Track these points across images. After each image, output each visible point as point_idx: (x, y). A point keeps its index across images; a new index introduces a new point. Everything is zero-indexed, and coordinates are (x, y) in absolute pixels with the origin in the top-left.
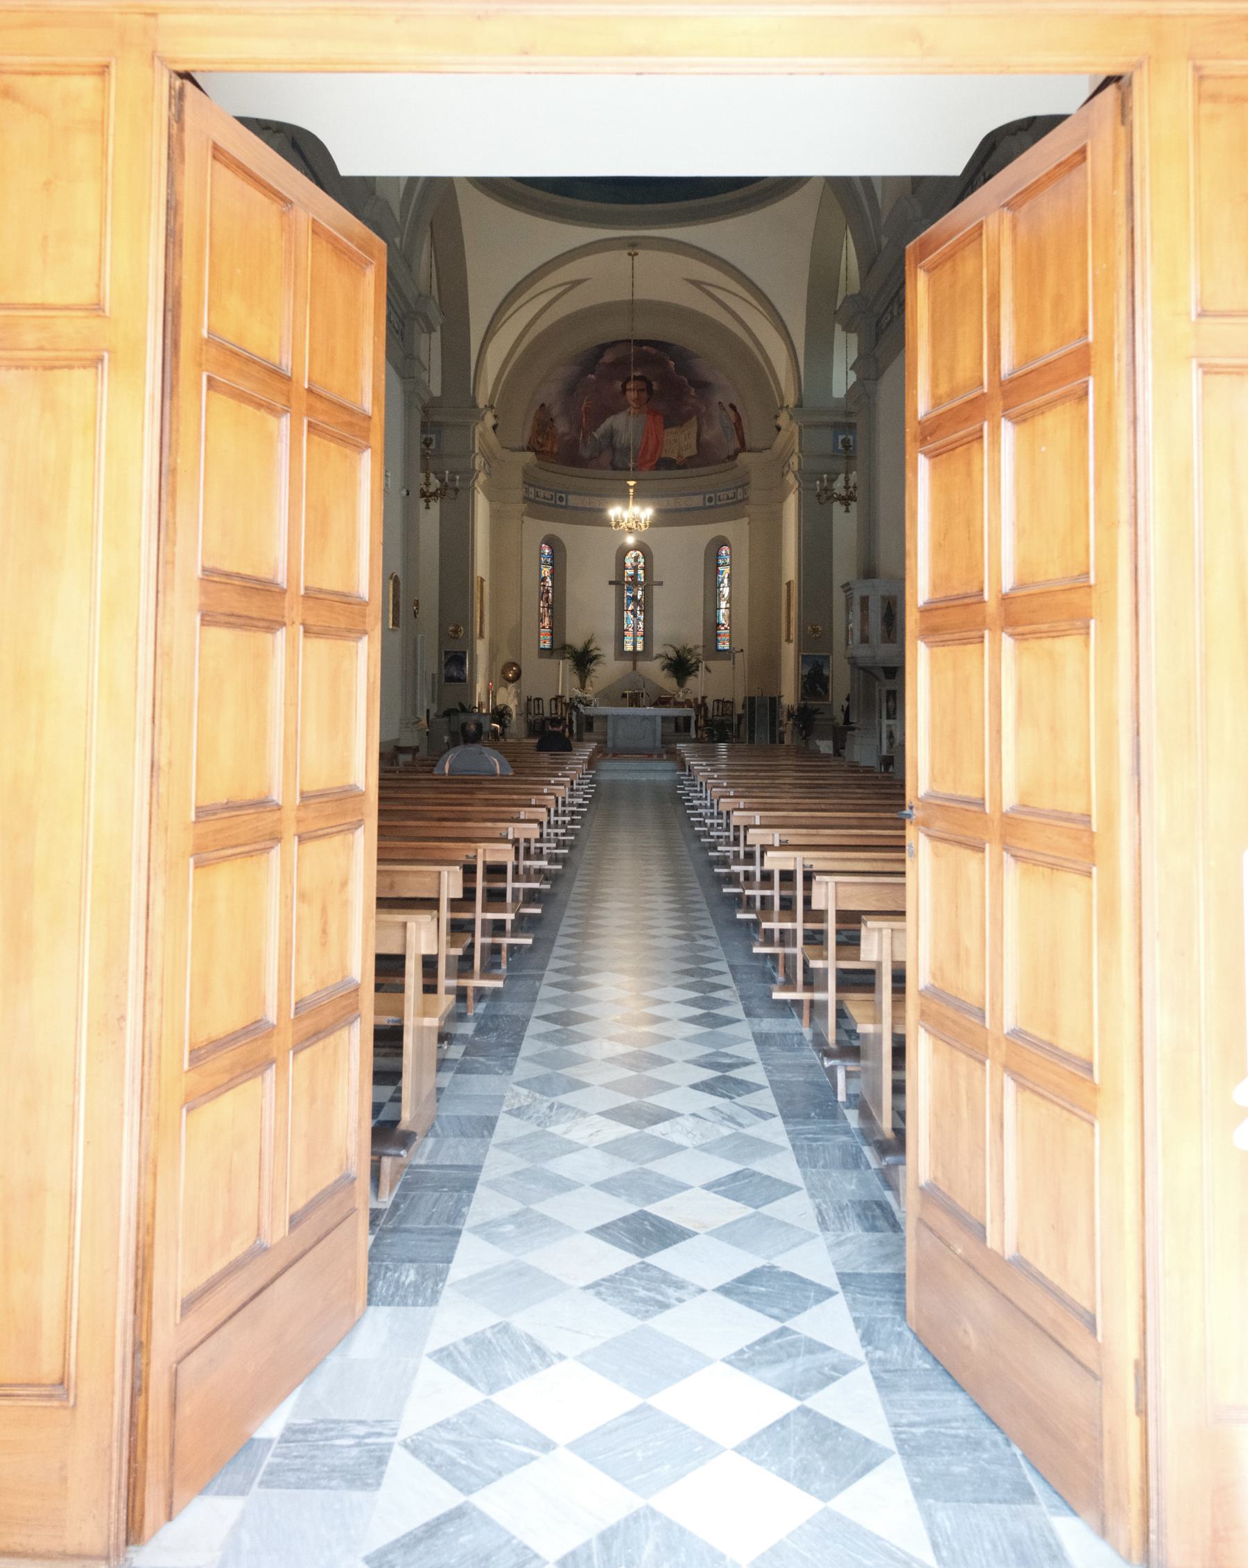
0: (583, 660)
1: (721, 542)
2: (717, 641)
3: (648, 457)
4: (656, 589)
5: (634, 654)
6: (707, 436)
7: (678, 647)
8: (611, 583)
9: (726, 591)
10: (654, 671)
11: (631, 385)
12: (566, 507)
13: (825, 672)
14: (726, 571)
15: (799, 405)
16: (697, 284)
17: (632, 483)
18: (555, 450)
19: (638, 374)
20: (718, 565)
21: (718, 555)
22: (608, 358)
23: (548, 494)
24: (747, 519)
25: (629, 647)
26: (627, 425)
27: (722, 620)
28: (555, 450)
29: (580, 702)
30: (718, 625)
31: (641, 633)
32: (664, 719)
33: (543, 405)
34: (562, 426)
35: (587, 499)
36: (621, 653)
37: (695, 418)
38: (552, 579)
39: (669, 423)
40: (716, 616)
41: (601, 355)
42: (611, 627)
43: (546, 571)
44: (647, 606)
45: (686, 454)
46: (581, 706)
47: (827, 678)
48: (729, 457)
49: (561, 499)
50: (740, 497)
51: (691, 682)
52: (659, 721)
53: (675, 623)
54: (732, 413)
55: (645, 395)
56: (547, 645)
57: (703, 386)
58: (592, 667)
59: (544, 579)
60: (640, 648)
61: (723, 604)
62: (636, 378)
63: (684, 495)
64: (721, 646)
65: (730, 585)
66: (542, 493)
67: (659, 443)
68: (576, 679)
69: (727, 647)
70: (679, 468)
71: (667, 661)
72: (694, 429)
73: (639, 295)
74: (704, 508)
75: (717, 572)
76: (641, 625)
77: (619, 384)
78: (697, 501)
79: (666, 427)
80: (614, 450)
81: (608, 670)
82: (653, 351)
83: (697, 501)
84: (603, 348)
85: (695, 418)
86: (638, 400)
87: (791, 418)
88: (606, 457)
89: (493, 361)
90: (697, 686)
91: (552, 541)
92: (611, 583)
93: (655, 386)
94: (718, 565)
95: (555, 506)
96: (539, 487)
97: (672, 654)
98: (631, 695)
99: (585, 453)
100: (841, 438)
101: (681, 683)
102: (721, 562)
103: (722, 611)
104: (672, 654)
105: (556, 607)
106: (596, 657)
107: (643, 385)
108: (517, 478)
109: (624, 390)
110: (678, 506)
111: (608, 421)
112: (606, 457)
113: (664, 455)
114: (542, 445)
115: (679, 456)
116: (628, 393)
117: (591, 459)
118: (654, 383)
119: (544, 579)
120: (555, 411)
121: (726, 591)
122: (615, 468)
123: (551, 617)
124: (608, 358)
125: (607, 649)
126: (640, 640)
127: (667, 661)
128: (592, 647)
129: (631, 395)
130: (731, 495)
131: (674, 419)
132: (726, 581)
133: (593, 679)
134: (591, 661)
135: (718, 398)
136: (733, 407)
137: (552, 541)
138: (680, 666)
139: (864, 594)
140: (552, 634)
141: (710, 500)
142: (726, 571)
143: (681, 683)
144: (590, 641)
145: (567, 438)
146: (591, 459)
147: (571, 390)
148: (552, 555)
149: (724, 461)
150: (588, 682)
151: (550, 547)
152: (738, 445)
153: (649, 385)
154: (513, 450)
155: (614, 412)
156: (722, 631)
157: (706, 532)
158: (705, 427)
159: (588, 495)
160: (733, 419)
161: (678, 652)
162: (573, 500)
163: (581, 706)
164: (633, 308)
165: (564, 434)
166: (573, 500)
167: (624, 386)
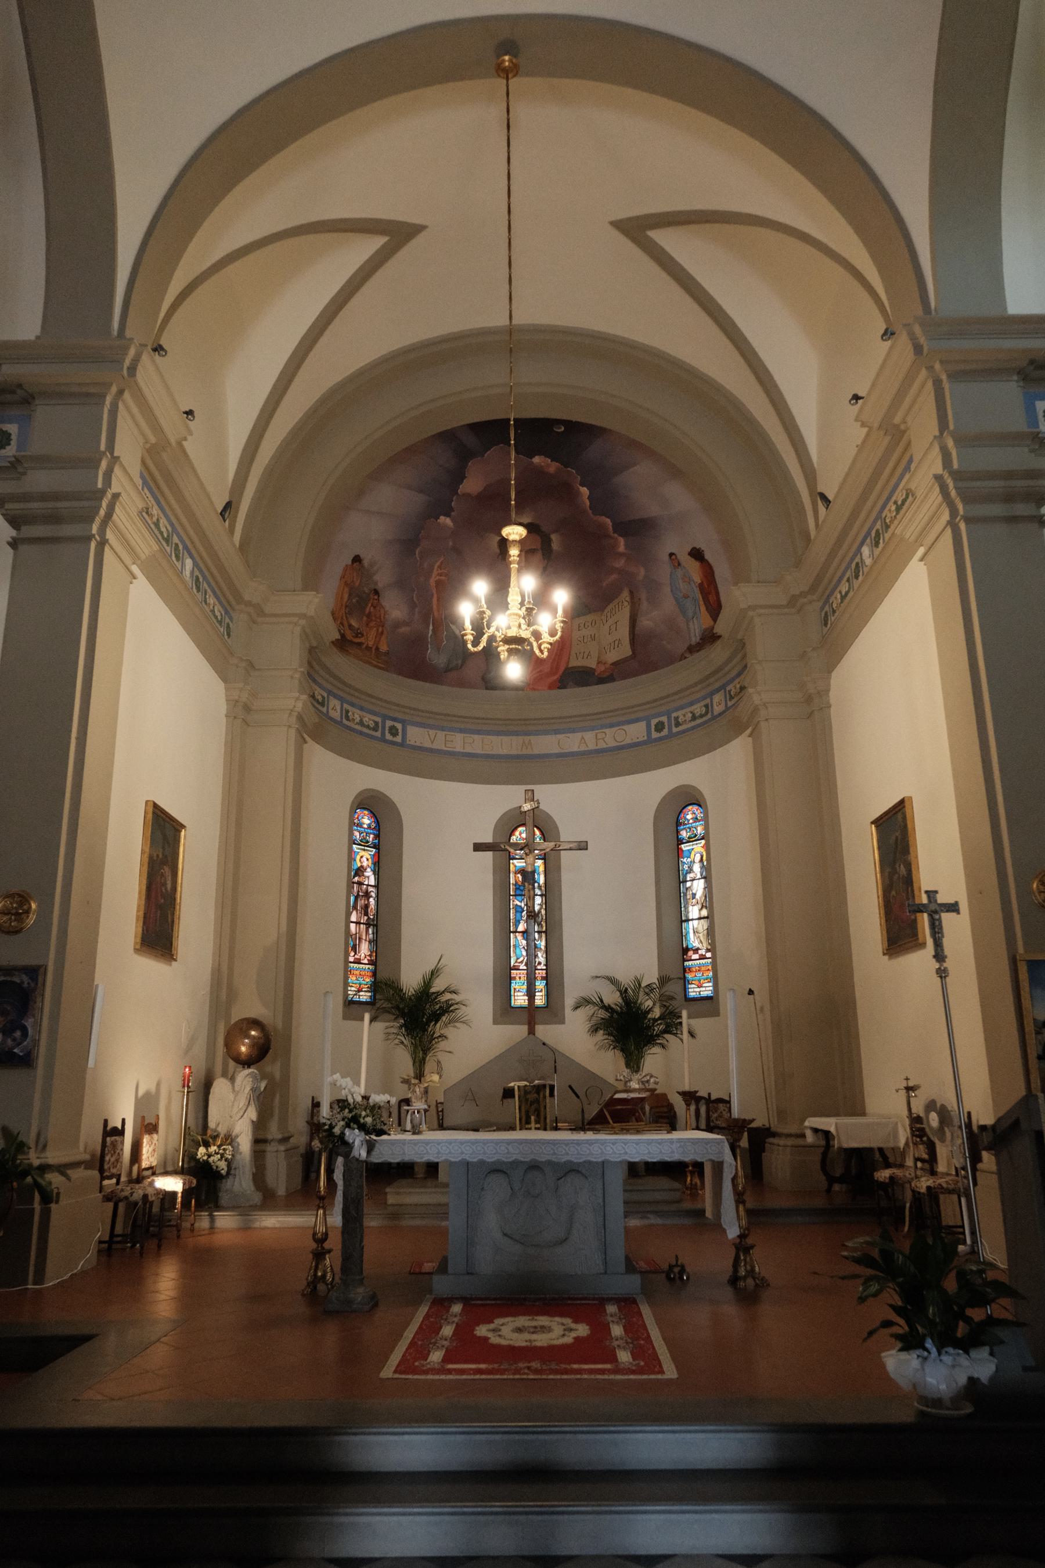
0: (417, 1014)
2: (685, 982)
5: (531, 1015)
6: (646, 623)
7: (625, 978)
8: (478, 847)
10: (576, 1038)
12: (402, 745)
14: (697, 849)
20: (680, 842)
21: (678, 824)
23: (368, 719)
25: (520, 999)
27: (693, 941)
28: (384, 648)
29: (354, 1121)
30: (686, 950)
31: (540, 973)
32: (635, 1170)
33: (357, 559)
35: (441, 735)
36: (505, 1011)
37: (625, 594)
38: (377, 873)
40: (682, 936)
41: (459, 476)
42: (485, 960)
43: (364, 857)
44: (549, 923)
45: (612, 657)
46: (355, 1137)
49: (394, 731)
50: (717, 709)
51: (653, 1060)
52: (616, 1180)
53: (606, 944)
54: (693, 568)
57: (638, 530)
58: (438, 1028)
60: (540, 1000)
61: (694, 912)
63: (611, 726)
64: (693, 991)
65: (707, 878)
66: (356, 714)
68: (403, 1060)
69: (707, 990)
70: (601, 681)
71: (602, 1014)
73: (521, 318)
74: (649, 741)
75: (679, 853)
76: (541, 958)
78: (636, 731)
81: (474, 1041)
83: (636, 731)
85: (625, 594)
87: (918, 349)
90: (670, 1066)
92: (478, 847)
94: (680, 842)
95: (383, 740)
96: (352, 705)
97: (612, 998)
98: (524, 1091)
101: (633, 1063)
102: (684, 834)
106: (447, 1009)
108: (286, 651)
110: (602, 745)
113: (574, 663)
114: (358, 634)
115: (599, 662)
117: (447, 670)
120: (383, 577)
121: (698, 887)
123: (374, 942)
125: (477, 1003)
126: (540, 985)
127: (602, 1014)
128: (438, 986)
130: (698, 709)
132: (697, 868)
133: (441, 1056)
134: (436, 1017)
136: (697, 554)
138: (631, 1024)
141: (660, 727)
142: (697, 849)
143: (633, 1063)
144: (434, 973)
145: (403, 630)
146: (447, 670)
148: (378, 829)
149: (683, 657)
150: (430, 1065)
151: (373, 815)
156: (694, 961)
157: (656, 784)
158: (644, 605)
160: (697, 578)
161: (624, 993)
162: (416, 735)
163: (355, 1137)
164: (514, 342)
165: (397, 625)
166: (416, 735)
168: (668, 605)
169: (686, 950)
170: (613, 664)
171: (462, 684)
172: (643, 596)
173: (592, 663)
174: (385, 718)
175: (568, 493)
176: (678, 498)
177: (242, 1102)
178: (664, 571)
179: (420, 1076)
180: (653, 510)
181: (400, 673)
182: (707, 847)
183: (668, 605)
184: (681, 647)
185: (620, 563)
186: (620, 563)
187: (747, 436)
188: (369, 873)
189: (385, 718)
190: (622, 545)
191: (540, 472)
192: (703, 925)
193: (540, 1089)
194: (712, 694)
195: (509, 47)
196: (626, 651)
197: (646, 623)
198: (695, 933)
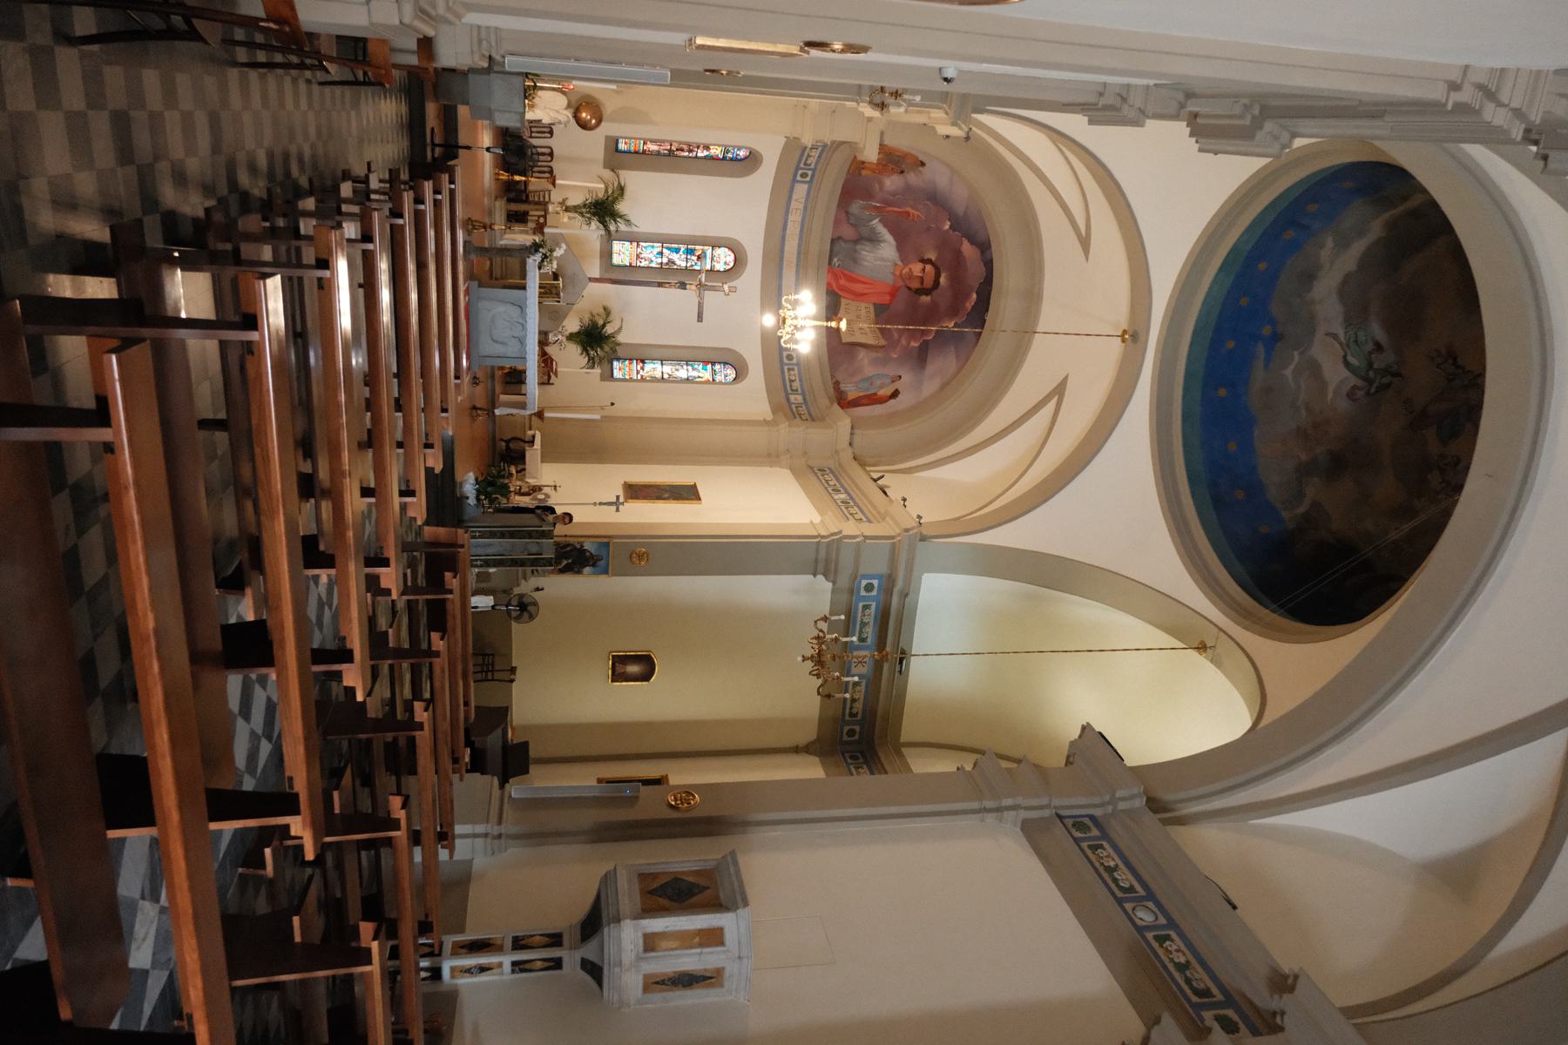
1: (741, 372)
3: (842, 282)
4: (690, 296)
6: (862, 354)
9: (682, 373)
11: (928, 267)
12: (794, 181)
13: (587, 570)
14: (706, 375)
15: (923, 539)
16: (1060, 390)
17: (843, 325)
19: (942, 280)
22: (967, 249)
23: (812, 161)
24: (770, 417)
26: (882, 259)
27: (649, 366)
28: (864, 172)
29: (545, 257)
30: (643, 362)
33: (923, 164)
34: (891, 182)
35: (801, 206)
41: (972, 241)
43: (716, 151)
47: (579, 572)
50: (792, 398)
51: (574, 350)
54: (888, 391)
55: (915, 285)
56: (622, 146)
57: (920, 357)
59: (707, 148)
61: (667, 369)
62: (938, 276)
67: (859, 296)
69: (617, 374)
71: (601, 322)
72: (870, 341)
75: (706, 363)
77: (932, 256)
80: (856, 242)
82: (969, 305)
84: (984, 247)
86: (910, 276)
87: (907, 530)
88: (848, 232)
89: (1019, 137)
90: (570, 358)
91: (752, 161)
93: (925, 299)
94: (713, 364)
95: (798, 168)
97: (609, 329)
98: (557, 287)
99: (856, 207)
100: (876, 583)
102: (717, 367)
103: (658, 365)
104: (609, 329)
105: (672, 159)
107: (929, 283)
109: (924, 261)
112: (848, 232)
113: (843, 302)
116: (919, 266)
117: (847, 213)
118: (928, 299)
119: (707, 148)
120: (912, 178)
121: (682, 373)
123: (658, 153)
124: (967, 249)
127: (601, 322)
129: (917, 268)
130: (796, 385)
132: (695, 374)
135: (907, 377)
136: (895, 394)
137: (752, 161)
138: (594, 339)
139: (729, 936)
140: (636, 152)
143: (571, 337)
147: (935, 199)
148: (735, 160)
149: (833, 377)
153: (927, 292)
154: (882, 133)
158: (874, 355)
159: (805, 208)
160: (881, 393)
162: (801, 190)
163: (538, 257)
165: (881, 184)
166: (801, 190)
167: (929, 261)
168: (869, 371)
169: (643, 362)
171: (837, 222)
174: (814, 170)
175: (954, 311)
176: (930, 387)
177: (553, 114)
178: (892, 371)
179: (567, 209)
180: (931, 368)
181: (846, 183)
182: (707, 382)
183: (869, 371)
184: (840, 377)
185: (904, 342)
186: (904, 342)
187: (945, 435)
188: (706, 153)
189: (814, 170)
190: (915, 344)
191: (967, 296)
192: (659, 375)
193: (558, 295)
194: (803, 394)
195: (1135, 337)
197: (862, 354)
198: (653, 369)
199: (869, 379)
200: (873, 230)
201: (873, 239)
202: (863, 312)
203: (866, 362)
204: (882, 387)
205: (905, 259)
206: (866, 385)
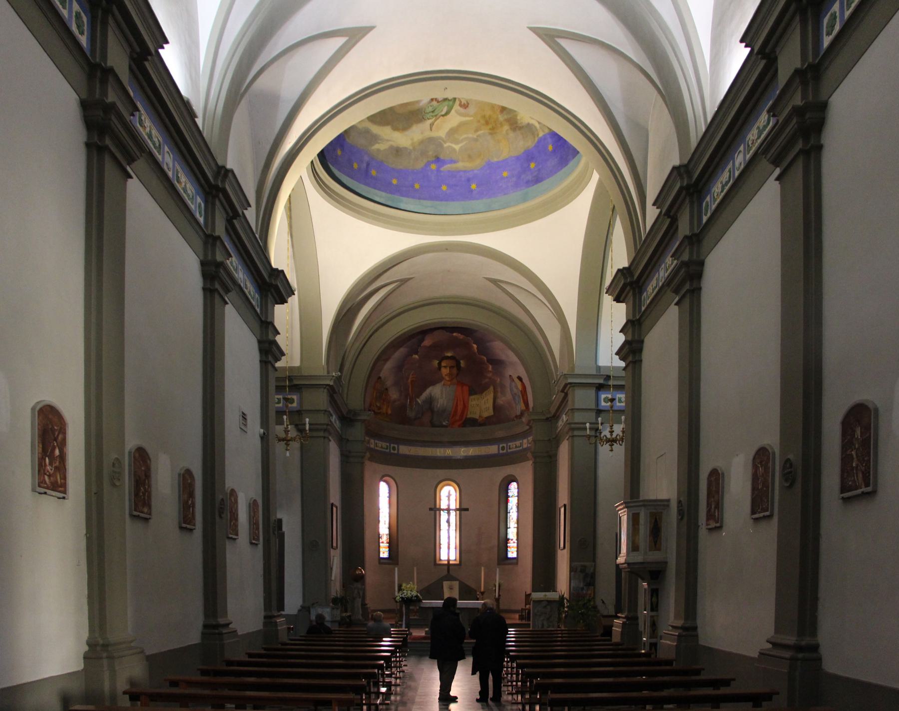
3: (457, 418)
6: (501, 401)
11: (443, 364)
18: (389, 412)
19: (449, 354)
26: (442, 393)
28: (389, 412)
34: (394, 395)
37: (492, 388)
39: (472, 392)
45: (485, 415)
48: (516, 417)
49: (394, 448)
55: (455, 371)
57: (498, 363)
62: (448, 358)
67: (465, 406)
70: (481, 425)
72: (492, 395)
77: (436, 362)
79: (470, 394)
85: (492, 388)
86: (450, 374)
93: (462, 363)
99: (411, 414)
111: (428, 391)
113: (469, 416)
114: (380, 408)
118: (462, 362)
120: (389, 383)
122: (433, 425)
129: (445, 371)
131: (477, 389)
135: (509, 372)
136: (520, 379)
141: (503, 448)
149: (513, 420)
152: (524, 408)
153: (458, 363)
155: (433, 383)
158: (499, 394)
160: (520, 387)
165: (395, 401)
167: (440, 364)
168: (509, 396)
170: (487, 418)
172: (499, 390)
173: (477, 416)
178: (507, 383)
180: (503, 357)
185: (490, 375)
196: (491, 412)
199: (514, 395)
200: (424, 402)
201: (430, 401)
202: (474, 403)
203: (503, 398)
204: (517, 388)
205: (441, 379)
206: (517, 398)
